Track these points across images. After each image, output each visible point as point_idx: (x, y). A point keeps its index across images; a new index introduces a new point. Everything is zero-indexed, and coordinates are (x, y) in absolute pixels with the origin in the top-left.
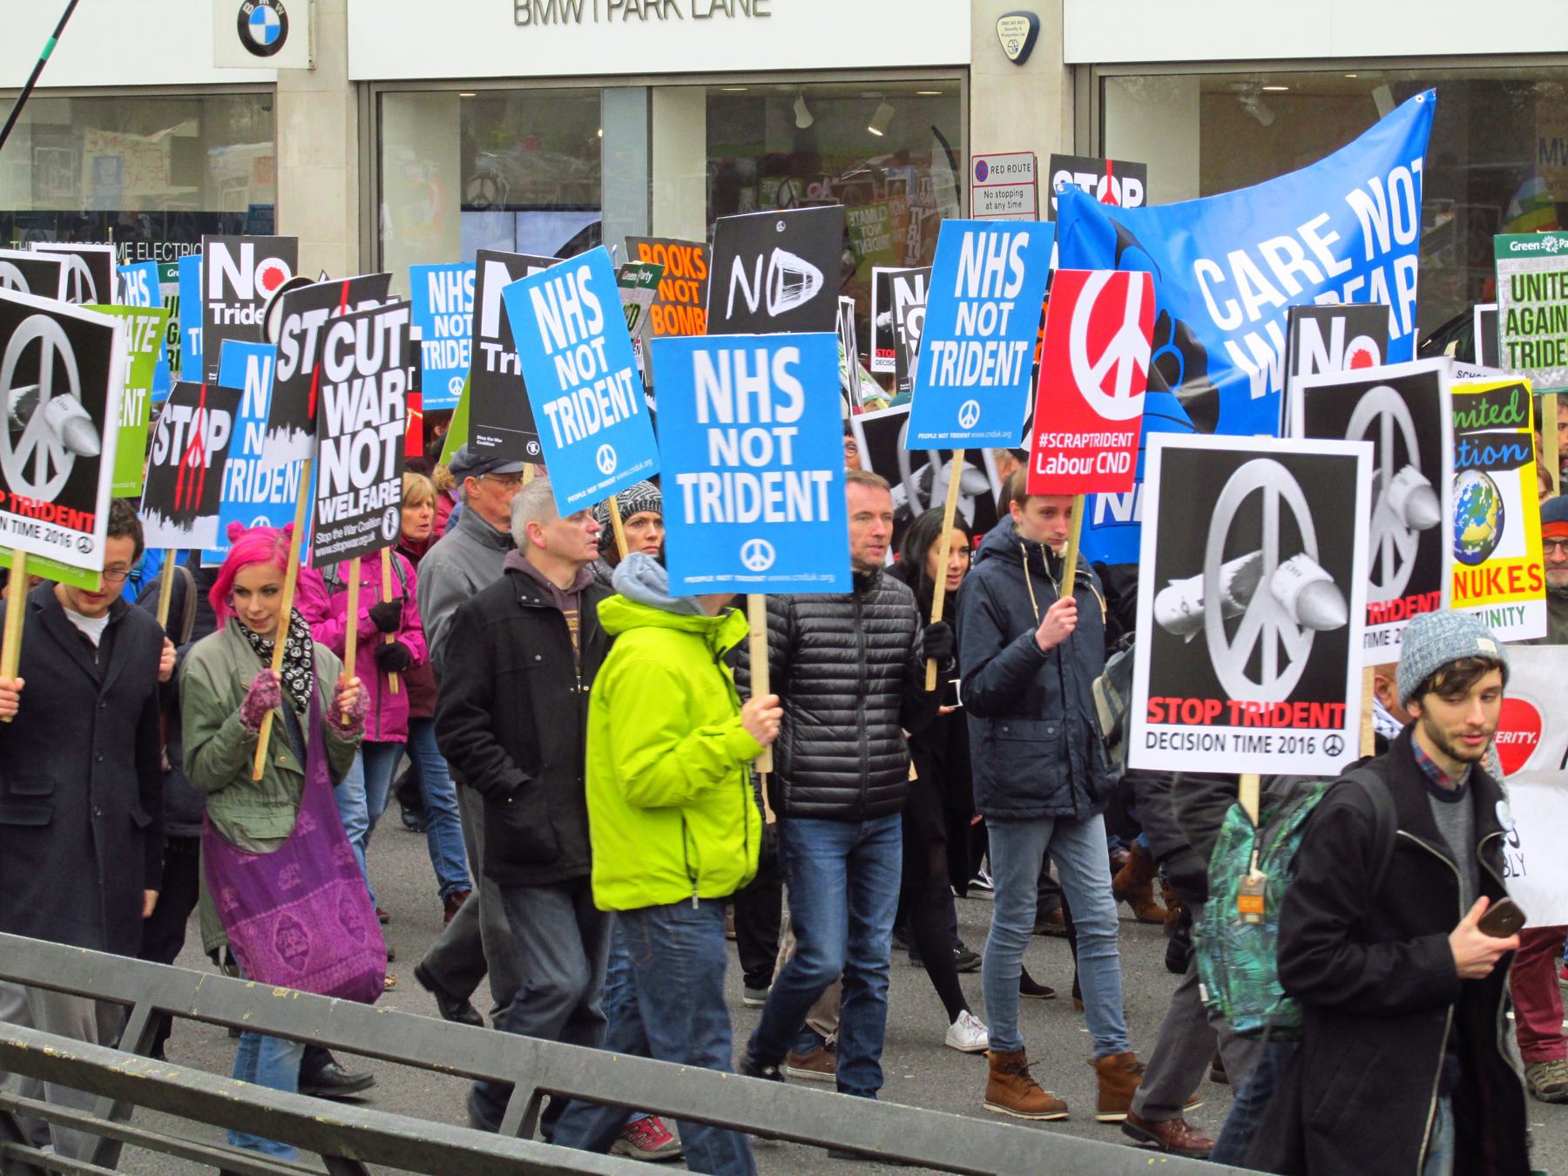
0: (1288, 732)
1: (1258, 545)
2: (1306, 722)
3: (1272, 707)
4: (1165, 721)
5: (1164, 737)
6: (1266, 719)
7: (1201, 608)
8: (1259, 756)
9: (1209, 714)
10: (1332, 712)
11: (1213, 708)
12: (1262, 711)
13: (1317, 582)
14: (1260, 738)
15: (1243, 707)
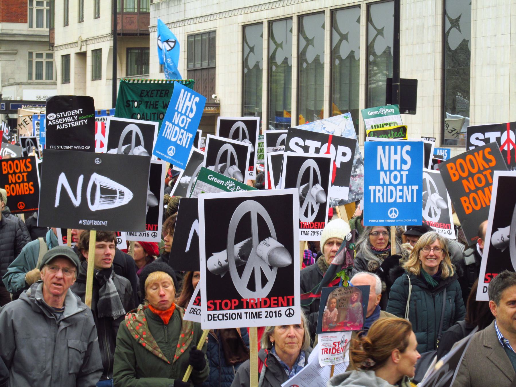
0: (269, 310)
1: (249, 234)
2: (277, 305)
3: (260, 300)
4: (215, 309)
5: (215, 316)
6: (259, 305)
7: (227, 263)
8: (257, 320)
9: (233, 305)
10: (288, 300)
11: (235, 302)
12: (256, 302)
13: (278, 248)
14: (256, 313)
15: (248, 301)
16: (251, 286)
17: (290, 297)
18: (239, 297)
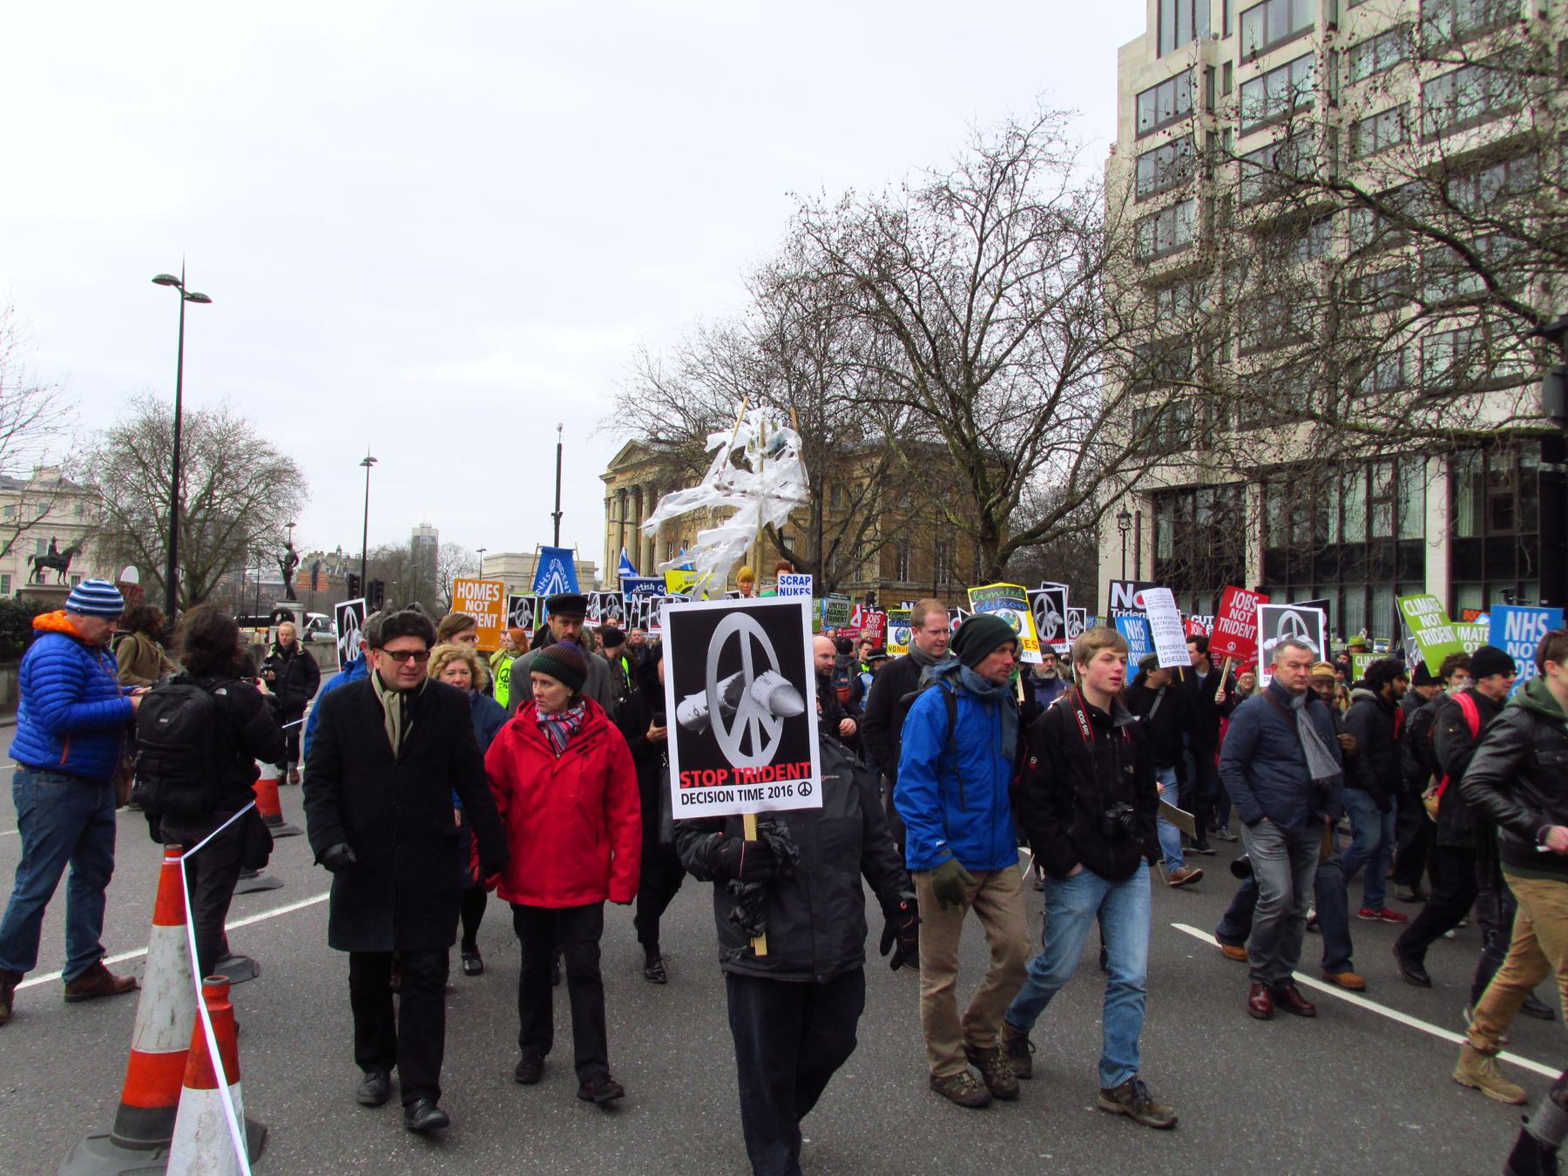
0: (773, 785)
1: (739, 666)
2: (785, 777)
4: (693, 785)
9: (720, 779)
10: (802, 769)
16: (746, 748)
17: (804, 765)
18: (727, 765)
